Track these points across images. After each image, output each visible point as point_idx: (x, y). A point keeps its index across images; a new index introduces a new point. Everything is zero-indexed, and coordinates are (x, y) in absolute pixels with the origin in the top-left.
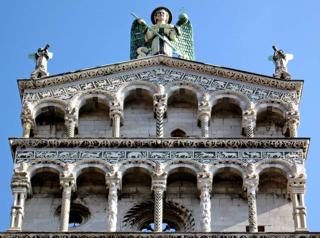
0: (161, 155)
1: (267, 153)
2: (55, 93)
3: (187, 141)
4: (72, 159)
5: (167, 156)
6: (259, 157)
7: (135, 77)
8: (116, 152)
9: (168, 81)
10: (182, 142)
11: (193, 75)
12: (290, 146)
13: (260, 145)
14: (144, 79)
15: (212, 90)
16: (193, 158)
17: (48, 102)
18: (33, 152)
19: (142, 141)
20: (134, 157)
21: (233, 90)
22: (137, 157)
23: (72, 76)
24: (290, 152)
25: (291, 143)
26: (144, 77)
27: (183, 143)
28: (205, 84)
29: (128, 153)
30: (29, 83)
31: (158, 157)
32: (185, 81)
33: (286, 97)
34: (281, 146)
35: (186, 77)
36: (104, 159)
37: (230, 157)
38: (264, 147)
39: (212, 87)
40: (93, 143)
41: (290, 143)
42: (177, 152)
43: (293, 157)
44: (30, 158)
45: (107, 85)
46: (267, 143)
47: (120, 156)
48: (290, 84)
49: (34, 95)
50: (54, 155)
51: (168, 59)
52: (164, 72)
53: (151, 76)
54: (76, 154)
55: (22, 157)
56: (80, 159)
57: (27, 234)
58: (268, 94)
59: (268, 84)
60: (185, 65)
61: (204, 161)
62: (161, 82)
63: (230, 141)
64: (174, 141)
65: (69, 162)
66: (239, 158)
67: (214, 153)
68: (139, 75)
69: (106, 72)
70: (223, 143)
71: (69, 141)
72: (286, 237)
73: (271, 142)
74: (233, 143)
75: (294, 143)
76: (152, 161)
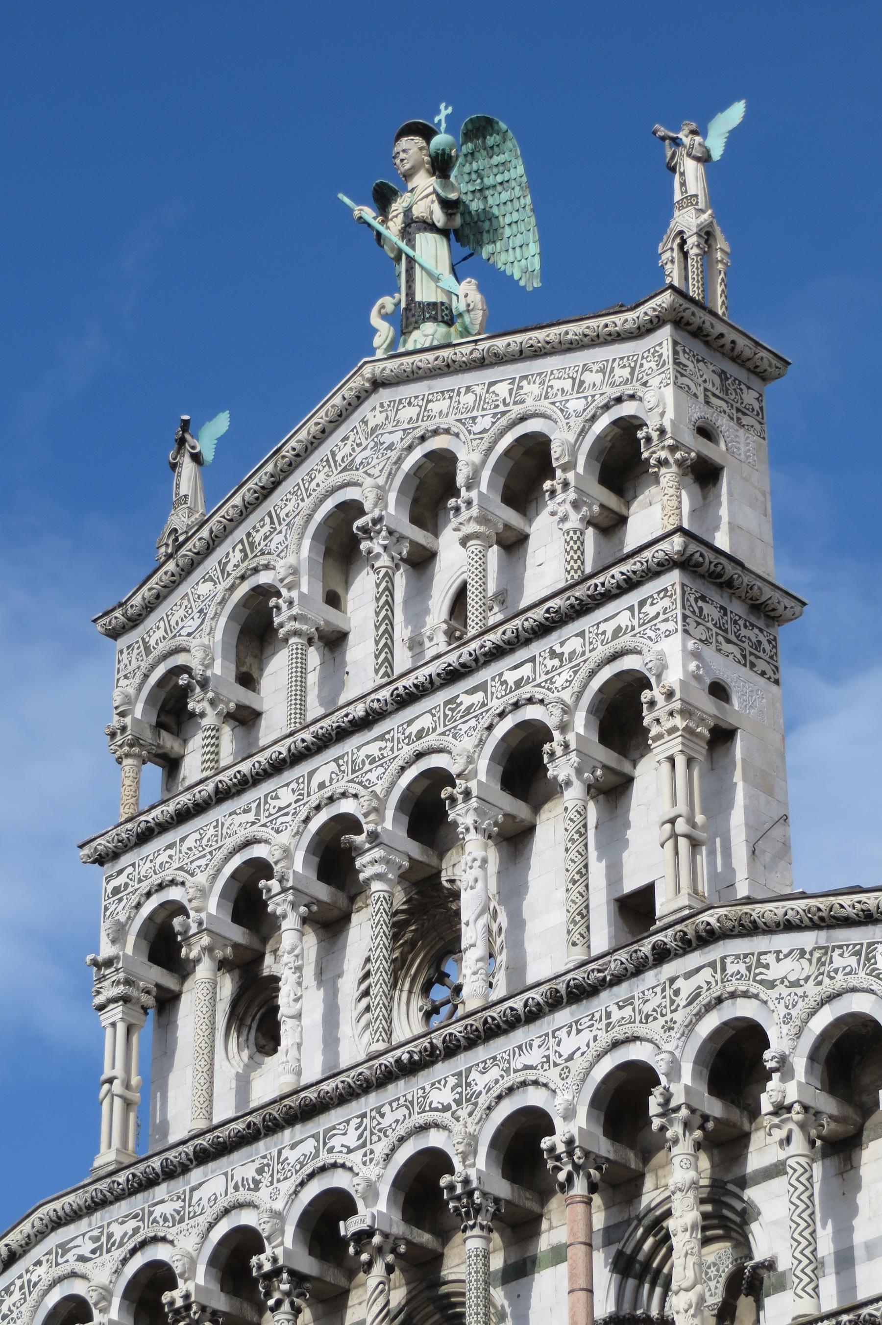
0: (373, 749)
1: (598, 624)
2: (173, 623)
4: (204, 856)
5: (390, 745)
7: (327, 469)
8: (287, 785)
9: (390, 447)
11: (442, 393)
13: (578, 608)
14: (343, 465)
15: (485, 431)
17: (165, 657)
18: (133, 865)
19: (326, 723)
21: (529, 402)
22: (327, 784)
23: (194, 546)
24: (652, 596)
26: (343, 461)
28: (470, 415)
29: (311, 774)
30: (116, 618)
31: (370, 764)
32: (428, 423)
33: (646, 365)
34: (624, 585)
35: (430, 406)
36: (264, 825)
37: (518, 684)
39: (483, 416)
40: (235, 780)
41: (639, 564)
42: (410, 723)
43: (658, 614)
44: (130, 889)
45: (271, 533)
46: (589, 593)
48: (642, 315)
49: (136, 651)
50: (170, 857)
51: (382, 367)
52: (384, 414)
53: (359, 445)
54: (212, 831)
55: (116, 891)
56: (220, 848)
57: (114, 1178)
58: (604, 374)
59: (601, 339)
60: (419, 368)
61: (464, 727)
65: (199, 867)
66: (538, 681)
67: (482, 687)
68: (333, 454)
69: (263, 488)
71: (188, 796)
75: (647, 562)
76: (359, 783)
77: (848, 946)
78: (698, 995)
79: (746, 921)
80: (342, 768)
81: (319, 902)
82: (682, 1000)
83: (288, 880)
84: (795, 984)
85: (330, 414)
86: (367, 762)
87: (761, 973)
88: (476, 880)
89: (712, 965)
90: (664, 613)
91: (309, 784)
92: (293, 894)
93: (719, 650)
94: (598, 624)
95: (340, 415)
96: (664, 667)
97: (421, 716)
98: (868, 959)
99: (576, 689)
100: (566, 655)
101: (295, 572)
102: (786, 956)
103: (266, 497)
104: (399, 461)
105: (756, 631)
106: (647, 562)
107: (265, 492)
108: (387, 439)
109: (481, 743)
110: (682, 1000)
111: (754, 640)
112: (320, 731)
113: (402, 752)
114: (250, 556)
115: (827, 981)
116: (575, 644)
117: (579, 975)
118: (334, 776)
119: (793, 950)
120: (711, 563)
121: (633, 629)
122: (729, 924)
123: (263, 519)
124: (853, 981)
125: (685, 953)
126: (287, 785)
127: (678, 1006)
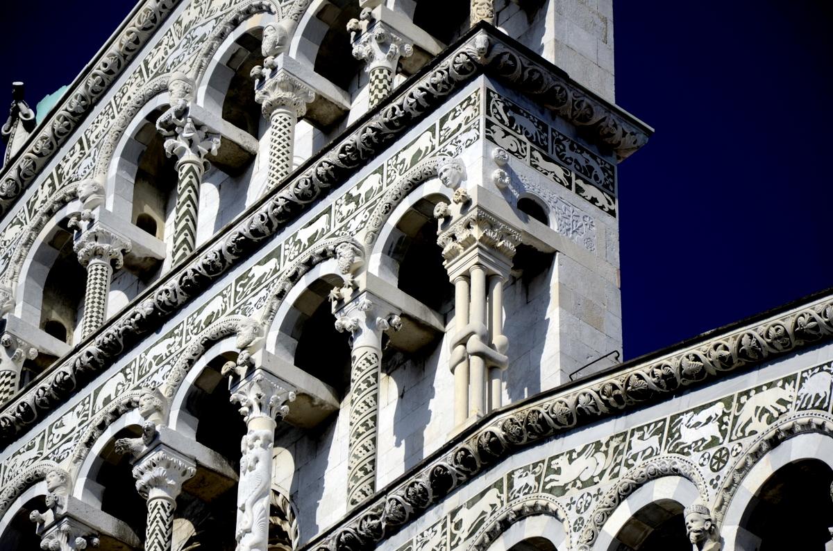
0: (161, 349)
1: (397, 155)
3: (206, 258)
6: (378, 186)
7: (139, 79)
8: (73, 409)
10: (197, 269)
12: (449, 86)
14: (155, 71)
16: (232, 308)
20: (107, 401)
25: (442, 73)
26: (155, 67)
27: (200, 269)
34: (424, 104)
36: (47, 458)
37: (312, 240)
38: (389, 137)
40: (18, 415)
41: (439, 75)
42: (199, 311)
43: (460, 125)
45: (80, 158)
46: (387, 119)
47: (81, 416)
61: (254, 300)
62: (189, 54)
63: (298, 183)
64: (179, 278)
67: (276, 254)
68: (146, 63)
69: (73, 113)
70: (287, 200)
72: (396, 500)
73: (394, 109)
74: (309, 181)
77: (648, 426)
78: (482, 521)
79: (533, 421)
80: (129, 377)
81: (101, 535)
82: (463, 533)
83: (61, 507)
84: (590, 482)
85: (143, 20)
86: (154, 363)
87: (551, 480)
88: (257, 461)
89: (498, 485)
90: (466, 123)
91: (94, 402)
92: (69, 523)
93: (536, 166)
94: (397, 155)
95: (154, 21)
96: (463, 178)
97: (212, 301)
98: (671, 435)
99: (372, 228)
100: (363, 196)
101: (100, 191)
102: (579, 455)
103: (78, 124)
104: (210, 52)
105: (588, 156)
106: (447, 70)
107: (76, 118)
108: (199, 33)
109: (272, 313)
110: (463, 533)
111: (583, 163)
112: (107, 340)
113: (190, 343)
114: (58, 187)
115: (624, 471)
116: (373, 182)
117: (351, 526)
118: (120, 387)
119: (587, 446)
120: (524, 69)
121: (433, 148)
122: (514, 429)
123: (73, 148)
124: (655, 464)
125: (470, 479)
126: (73, 409)
127: (460, 539)
